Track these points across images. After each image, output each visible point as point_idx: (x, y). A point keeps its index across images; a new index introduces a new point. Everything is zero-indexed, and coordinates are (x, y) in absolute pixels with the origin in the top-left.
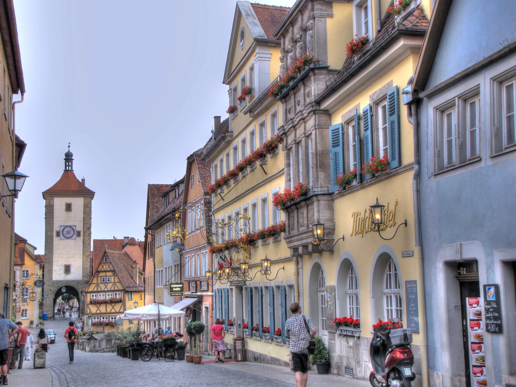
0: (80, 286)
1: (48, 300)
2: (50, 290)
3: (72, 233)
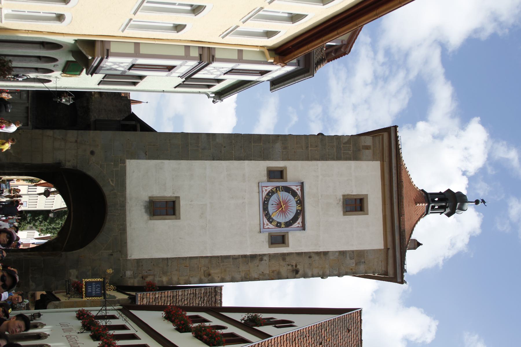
2: (92, 153)
3: (282, 219)
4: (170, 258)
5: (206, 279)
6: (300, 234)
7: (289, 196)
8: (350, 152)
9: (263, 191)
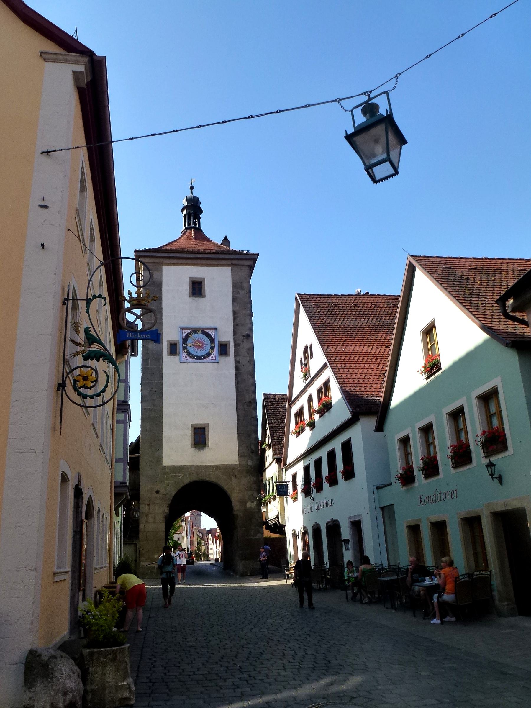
0: (234, 481)
1: (151, 520)
2: (157, 492)
9: (187, 360)
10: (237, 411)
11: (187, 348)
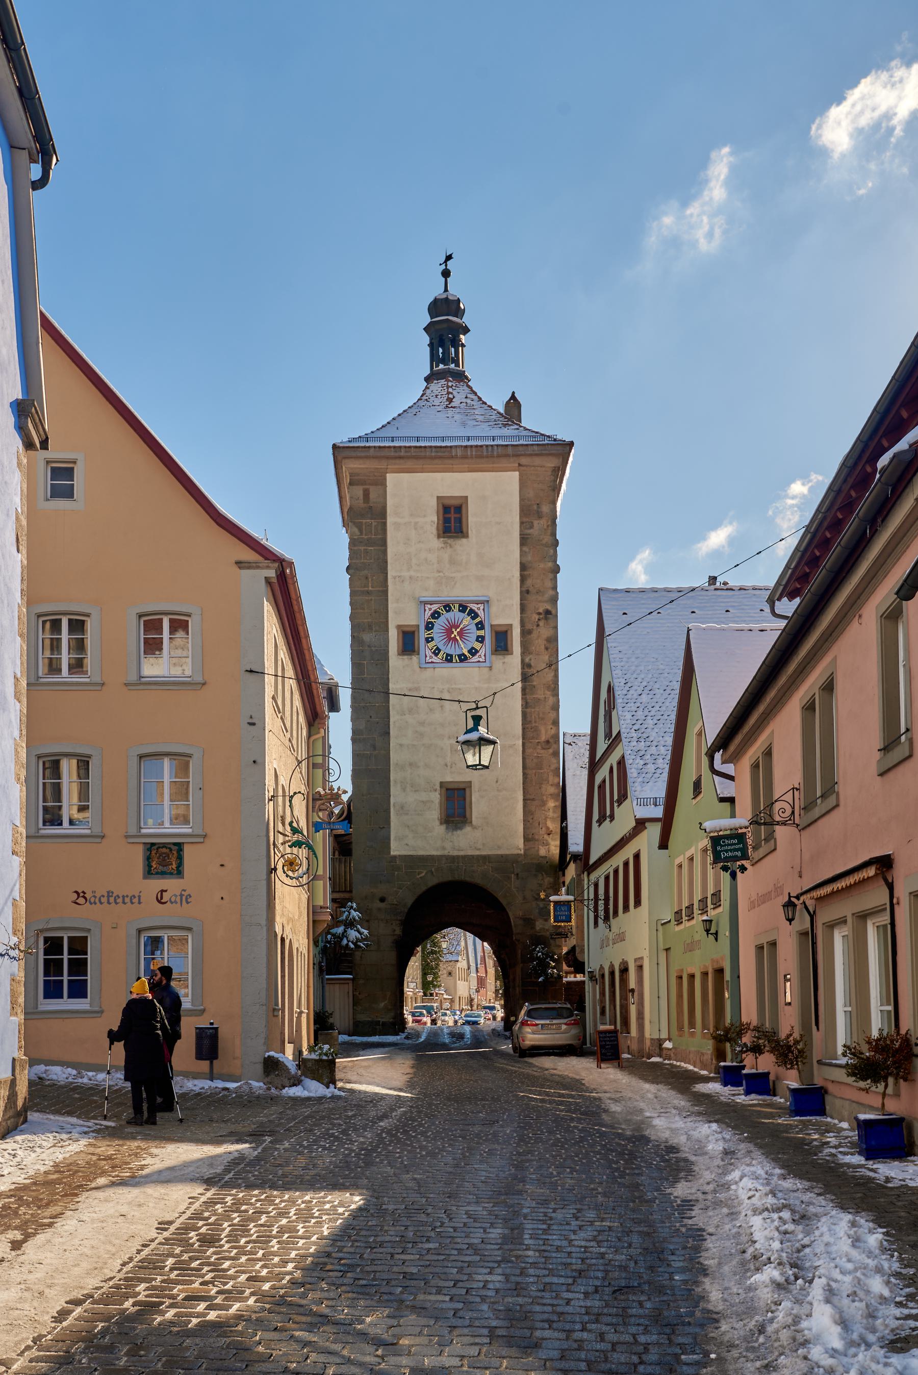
2: (382, 900)
3: (474, 633)
4: (524, 796)
5: (555, 746)
6: (494, 609)
7: (440, 623)
8: (374, 524)
9: (432, 662)
10: (524, 759)
11: (433, 639)
